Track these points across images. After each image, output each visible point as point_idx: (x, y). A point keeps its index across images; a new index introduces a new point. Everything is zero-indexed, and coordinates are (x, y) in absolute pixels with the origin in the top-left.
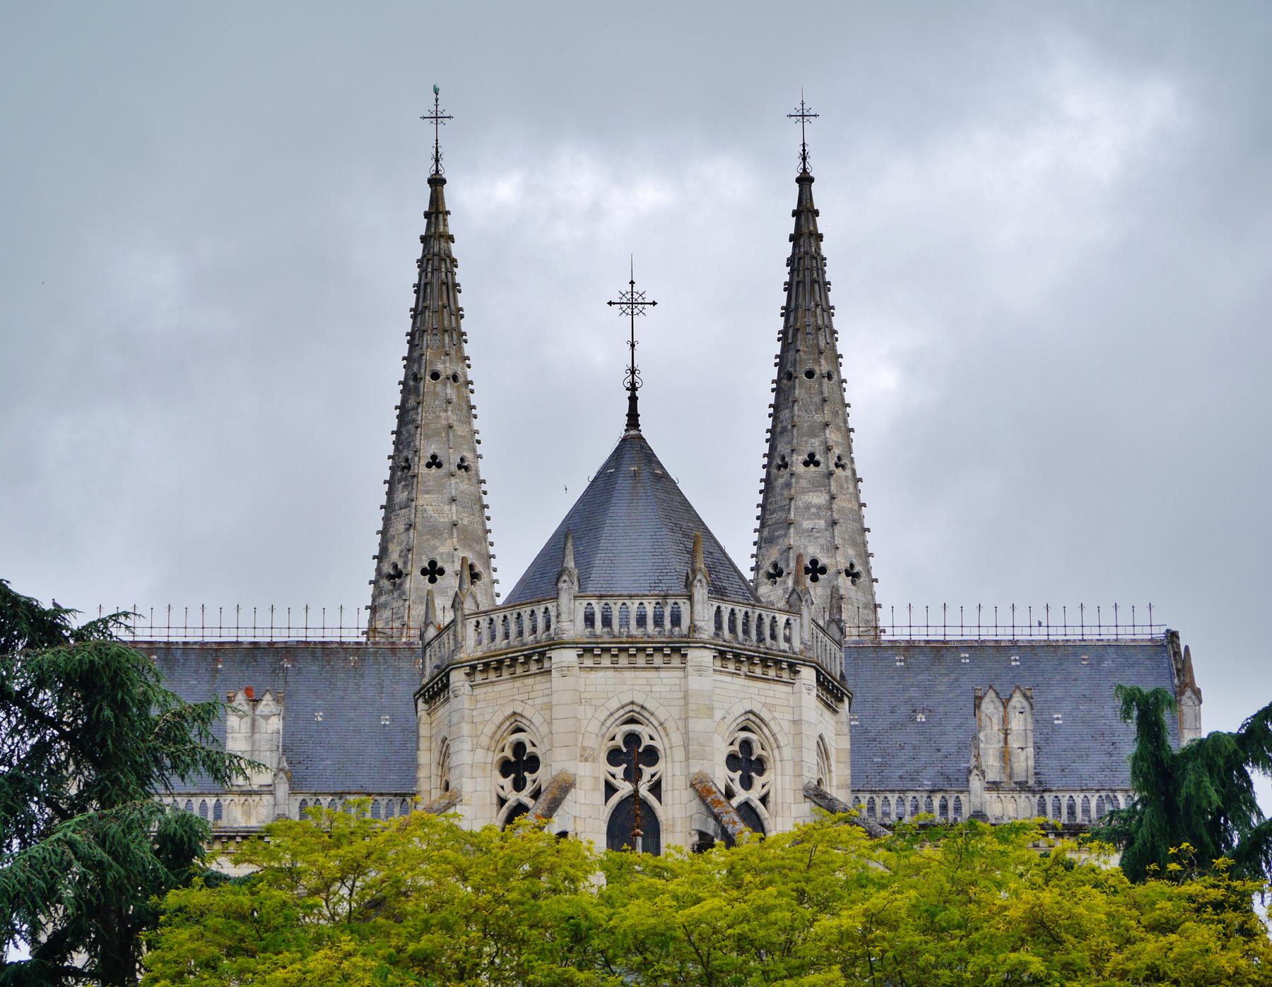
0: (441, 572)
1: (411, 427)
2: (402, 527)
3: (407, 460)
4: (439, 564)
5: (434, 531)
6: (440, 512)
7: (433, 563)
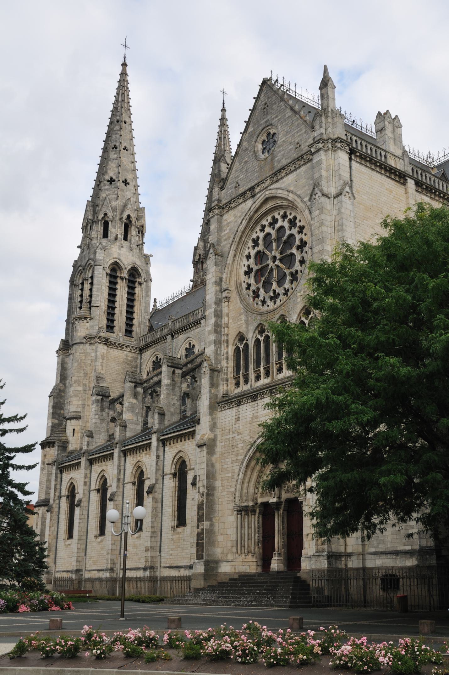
0: (128, 184)
1: (118, 136)
2: (115, 166)
3: (115, 146)
4: (128, 181)
5: (126, 170)
6: (128, 165)
7: (126, 180)
